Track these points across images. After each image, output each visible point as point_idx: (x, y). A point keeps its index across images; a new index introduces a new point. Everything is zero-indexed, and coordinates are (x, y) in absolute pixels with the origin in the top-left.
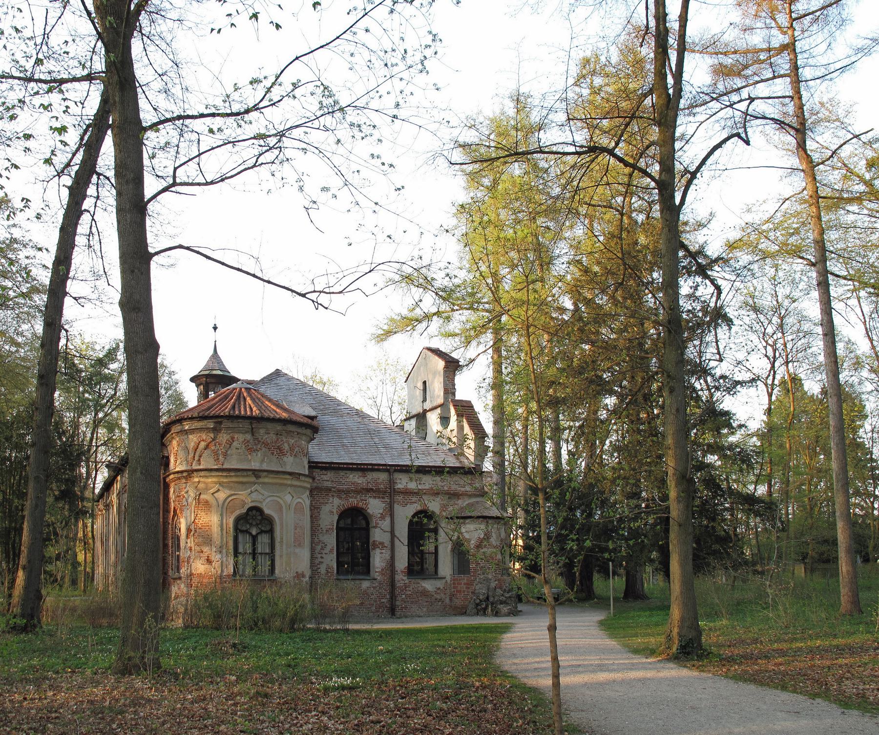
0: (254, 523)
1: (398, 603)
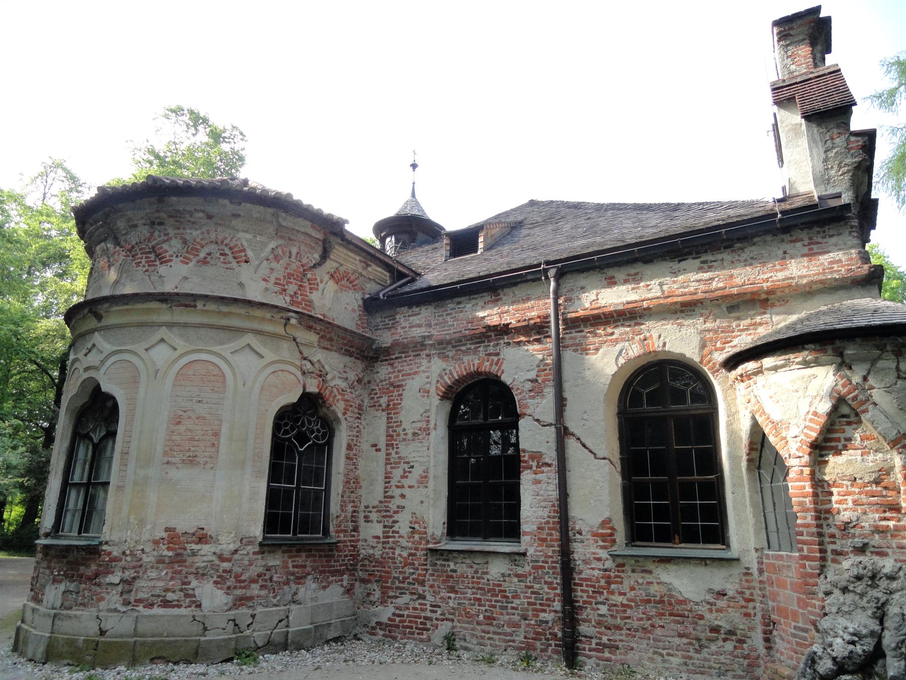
1: (583, 628)
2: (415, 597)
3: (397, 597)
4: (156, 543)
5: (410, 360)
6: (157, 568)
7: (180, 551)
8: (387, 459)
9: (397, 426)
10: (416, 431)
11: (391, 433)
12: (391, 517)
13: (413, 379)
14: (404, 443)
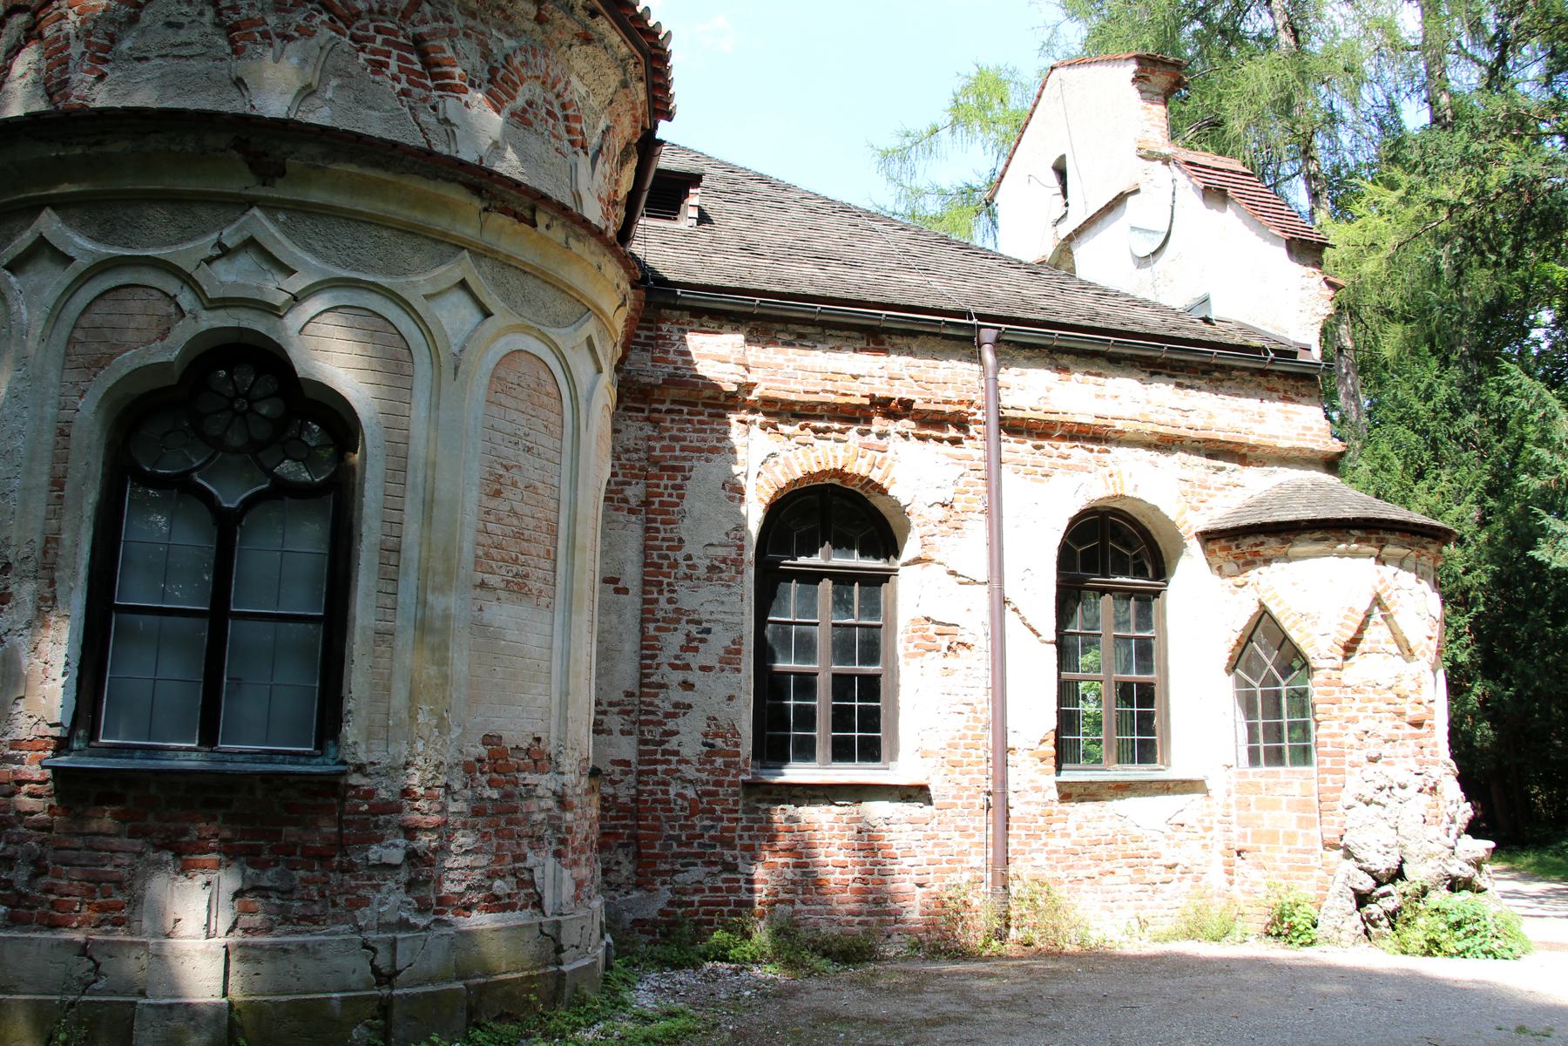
0: (235, 439)
2: (715, 869)
3: (675, 872)
4: (468, 768)
5: (700, 422)
6: (473, 827)
7: (509, 788)
8: (643, 611)
9: (669, 548)
10: (717, 563)
11: (656, 560)
12: (660, 723)
13: (707, 460)
14: (688, 583)
